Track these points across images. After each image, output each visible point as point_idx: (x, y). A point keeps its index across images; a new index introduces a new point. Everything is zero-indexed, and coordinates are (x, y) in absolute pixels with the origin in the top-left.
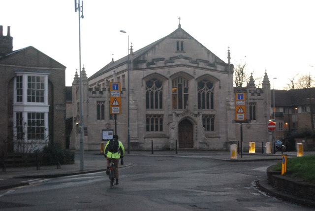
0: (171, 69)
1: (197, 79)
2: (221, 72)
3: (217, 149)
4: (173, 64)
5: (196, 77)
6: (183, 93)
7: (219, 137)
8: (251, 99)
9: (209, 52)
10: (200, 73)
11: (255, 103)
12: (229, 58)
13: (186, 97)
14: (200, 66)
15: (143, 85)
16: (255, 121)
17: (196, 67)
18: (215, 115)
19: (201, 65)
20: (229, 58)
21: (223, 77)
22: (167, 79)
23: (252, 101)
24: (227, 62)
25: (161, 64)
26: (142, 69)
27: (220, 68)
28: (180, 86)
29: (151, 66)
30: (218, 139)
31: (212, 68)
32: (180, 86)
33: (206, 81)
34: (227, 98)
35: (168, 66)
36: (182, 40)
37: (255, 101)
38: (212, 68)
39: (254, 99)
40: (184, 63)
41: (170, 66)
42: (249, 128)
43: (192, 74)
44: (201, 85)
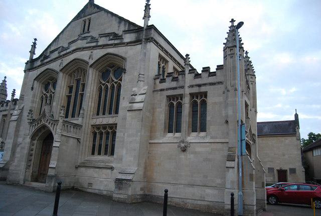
0: (66, 58)
1: (91, 66)
2: (128, 44)
3: (105, 193)
4: (68, 51)
5: (91, 62)
6: (73, 94)
7: (112, 168)
8: (192, 86)
9: (121, 19)
10: (98, 53)
11: (205, 94)
12: (147, 16)
13: (82, 95)
14: (100, 44)
15: (32, 88)
16: (203, 134)
17: (94, 47)
18: (117, 124)
19: (102, 41)
20: (147, 16)
21: (130, 53)
22: (57, 73)
23: (195, 90)
24: (141, 23)
25: (55, 55)
26: (35, 68)
27: (128, 38)
28: (78, 81)
29: (46, 61)
30: (109, 171)
31: (116, 42)
32: (78, 81)
33: (113, 66)
34: (134, 89)
35: (61, 56)
36: (89, 17)
37: (203, 89)
38: (116, 42)
39: (199, 86)
40: (79, 46)
41: (64, 55)
42: (184, 150)
43: (86, 58)
44: (104, 75)
